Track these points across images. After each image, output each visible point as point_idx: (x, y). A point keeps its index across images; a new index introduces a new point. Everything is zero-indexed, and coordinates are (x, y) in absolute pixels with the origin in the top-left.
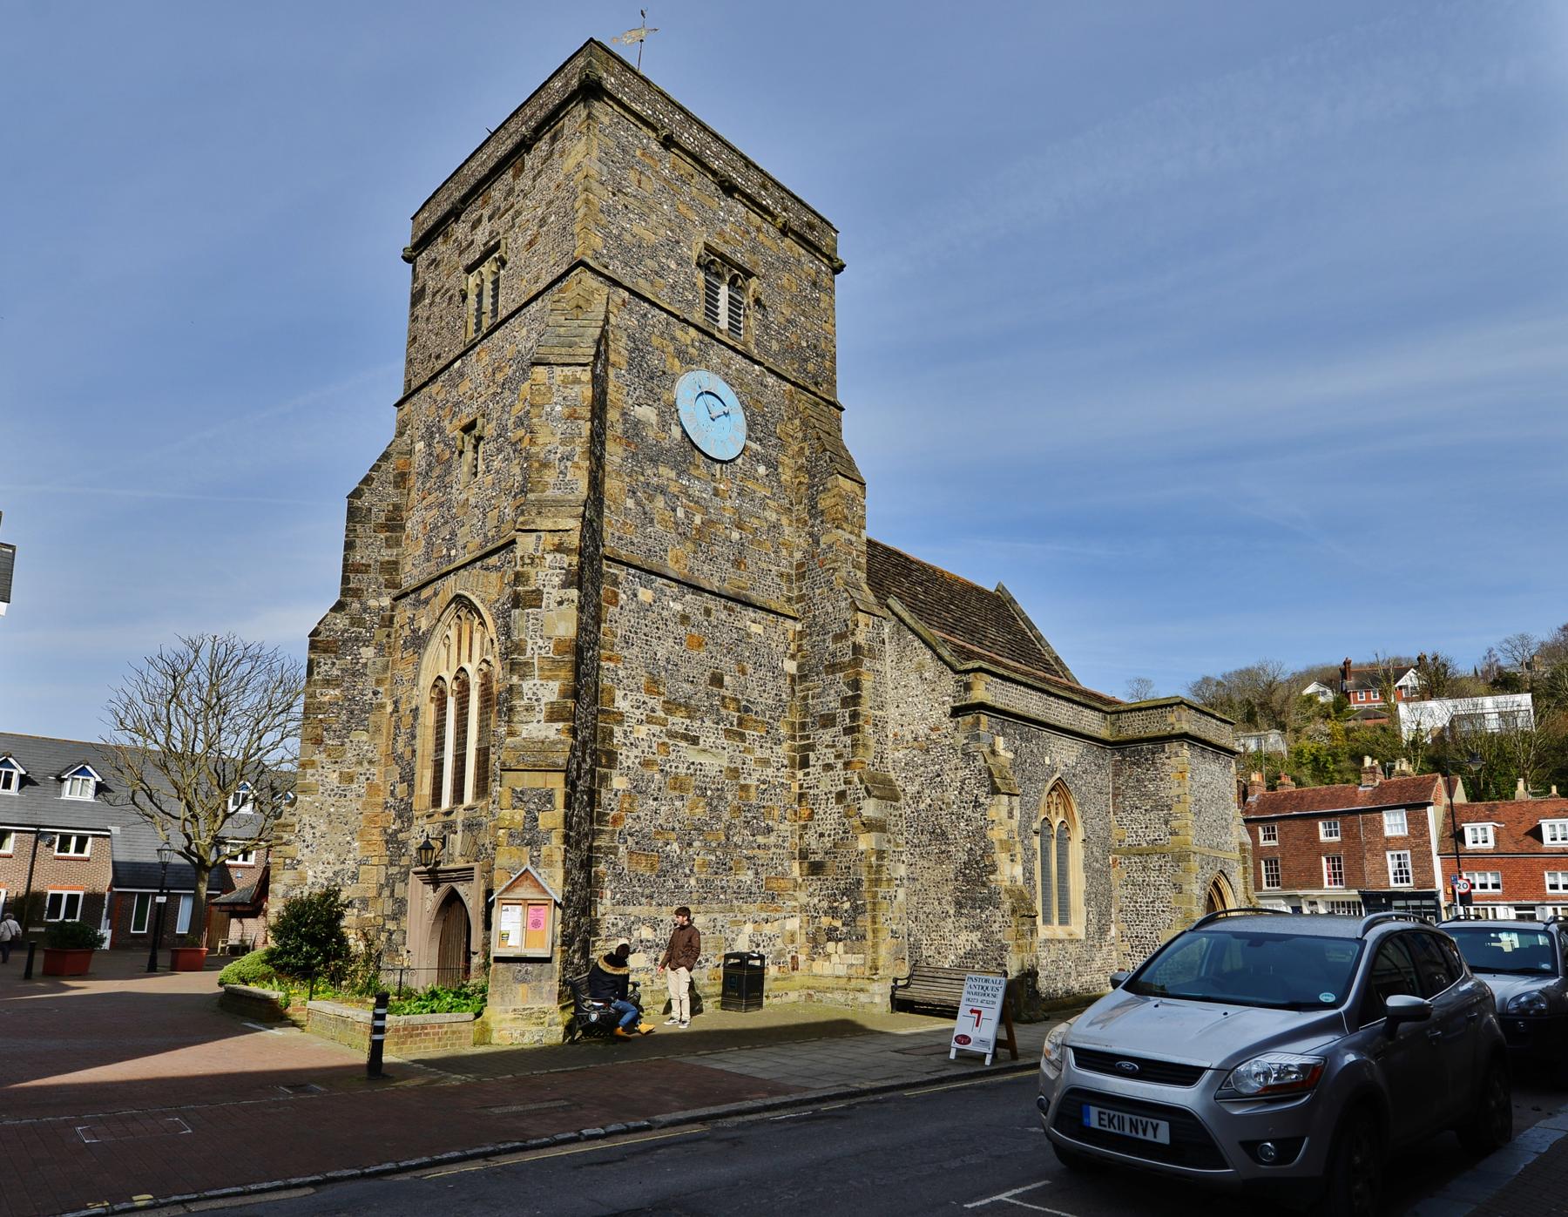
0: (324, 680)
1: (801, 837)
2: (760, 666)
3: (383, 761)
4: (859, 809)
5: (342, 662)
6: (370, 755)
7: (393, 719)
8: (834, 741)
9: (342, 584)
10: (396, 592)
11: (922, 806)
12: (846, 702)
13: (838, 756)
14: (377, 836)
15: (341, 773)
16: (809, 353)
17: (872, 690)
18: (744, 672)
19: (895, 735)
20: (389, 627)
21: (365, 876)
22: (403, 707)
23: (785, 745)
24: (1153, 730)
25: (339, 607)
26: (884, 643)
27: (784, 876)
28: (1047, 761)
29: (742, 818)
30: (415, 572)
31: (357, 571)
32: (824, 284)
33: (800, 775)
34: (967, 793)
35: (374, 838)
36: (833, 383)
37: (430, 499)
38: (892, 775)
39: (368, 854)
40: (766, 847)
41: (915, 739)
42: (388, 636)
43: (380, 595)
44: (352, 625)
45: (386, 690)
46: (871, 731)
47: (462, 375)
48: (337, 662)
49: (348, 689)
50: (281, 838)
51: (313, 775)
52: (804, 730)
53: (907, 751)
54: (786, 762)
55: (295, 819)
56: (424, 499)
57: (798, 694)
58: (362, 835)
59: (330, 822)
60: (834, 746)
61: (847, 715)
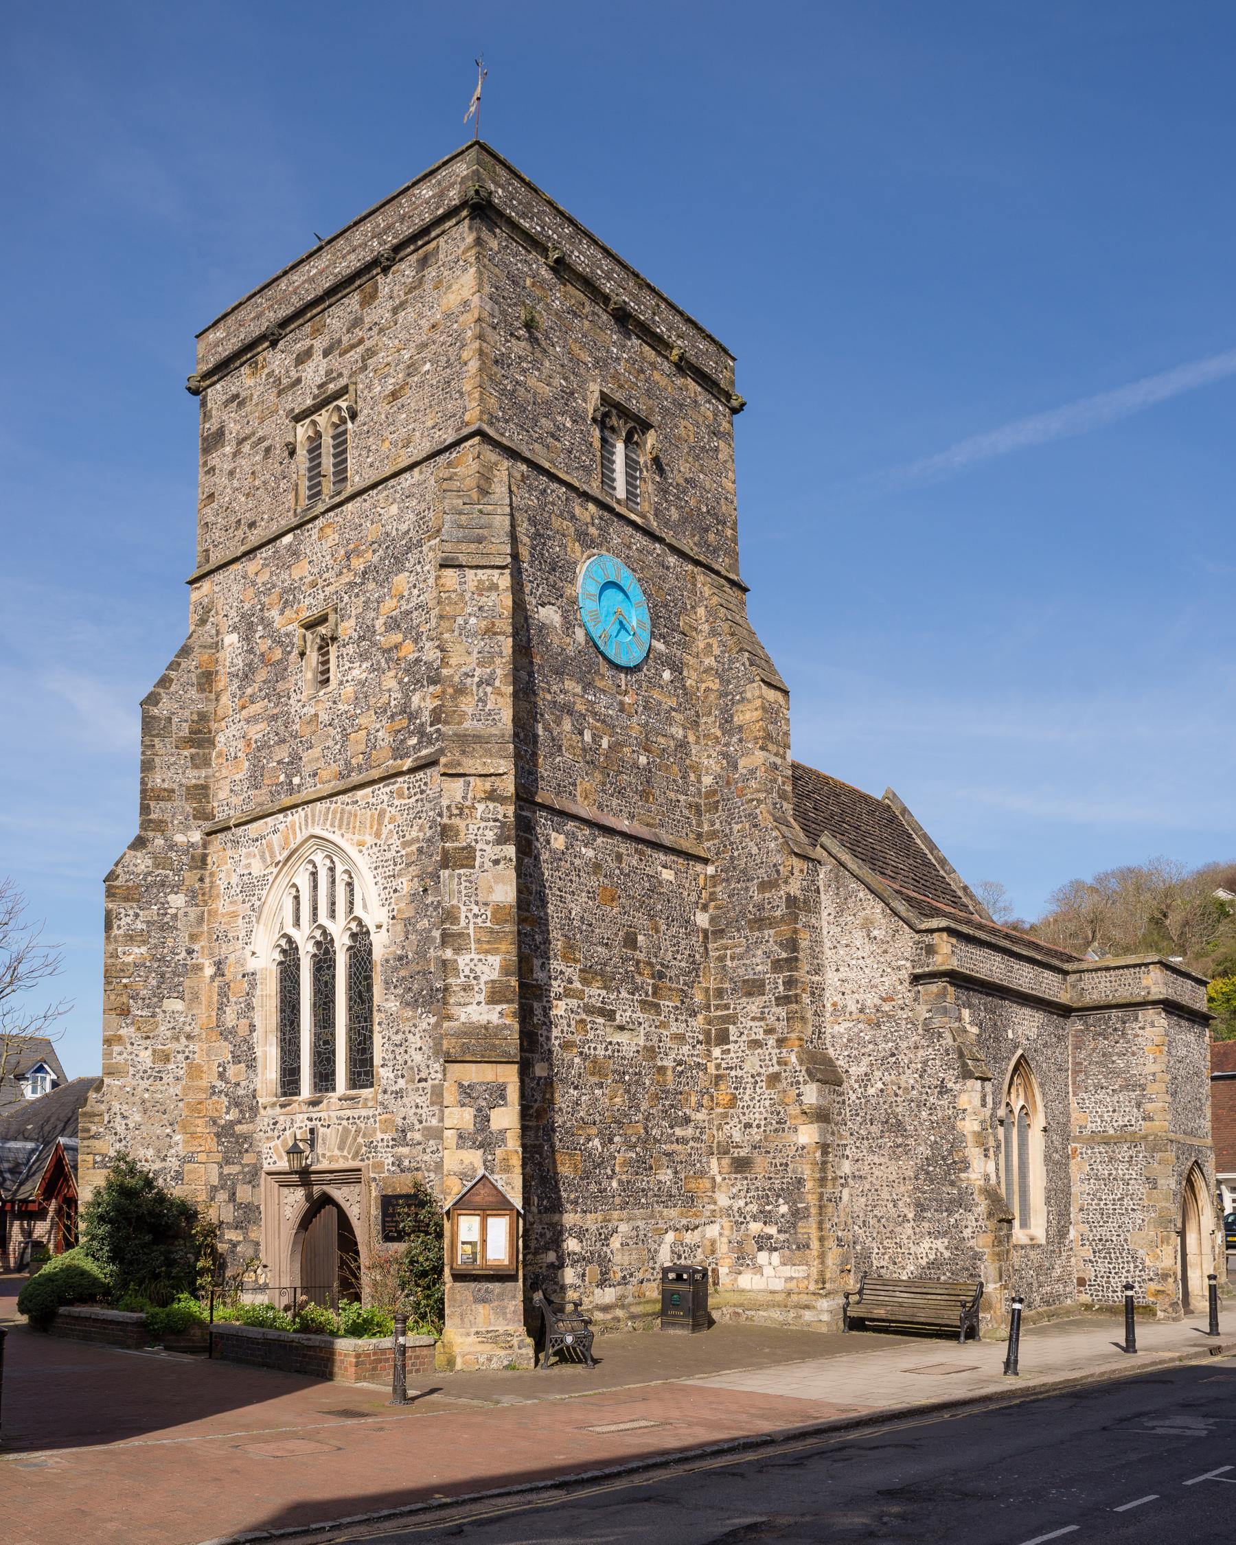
0: (126, 935)
1: (720, 1128)
2: (673, 921)
3: (204, 1036)
4: (798, 1095)
5: (147, 912)
6: (188, 1028)
7: (216, 984)
8: (763, 1013)
9: (141, 814)
10: (208, 826)
11: (871, 1091)
12: (777, 966)
13: (769, 1031)
14: (201, 1127)
15: (154, 1051)
16: (709, 520)
17: (809, 951)
18: (657, 931)
19: (834, 1005)
20: (202, 868)
21: (191, 1177)
22: (230, 972)
23: (700, 1017)
24: (1124, 995)
25: (139, 843)
26: (819, 893)
27: (702, 1174)
28: (1011, 1036)
29: (660, 1107)
30: (235, 800)
31: (158, 799)
32: (722, 429)
33: (717, 1052)
34: (929, 1076)
36: (733, 555)
38: (831, 1051)
39: (193, 1149)
40: (683, 1141)
41: (861, 1011)
42: (201, 880)
43: (188, 828)
44: (157, 866)
45: (202, 947)
46: (808, 1001)
47: (295, 554)
48: (141, 913)
49: (156, 947)
50: (88, 1130)
51: (120, 1054)
52: (722, 998)
53: (851, 1025)
54: (701, 1037)
55: (103, 1107)
56: (244, 707)
57: (711, 954)
58: (184, 1127)
59: (145, 1112)
60: (762, 1019)
61: (780, 981)
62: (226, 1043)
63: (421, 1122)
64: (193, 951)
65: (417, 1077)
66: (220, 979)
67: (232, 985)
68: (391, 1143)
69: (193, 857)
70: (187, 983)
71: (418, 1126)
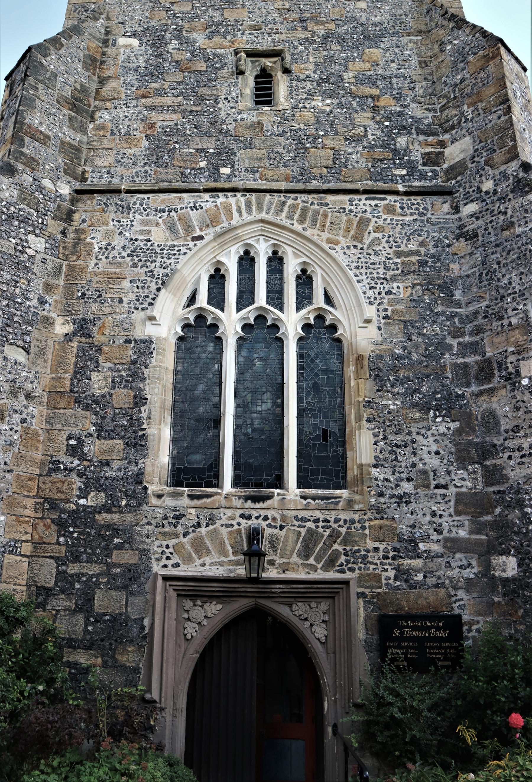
10: (78, 186)
20: (66, 222)
21: (10, 573)
35: (27, 512)
37: (168, 101)
39: (17, 536)
44: (23, 200)
56: (144, 96)
62: (88, 413)
63: (439, 531)
64: (46, 302)
65: (433, 483)
66: (83, 339)
67: (105, 349)
68: (391, 554)
69: (59, 207)
70: (35, 334)
71: (435, 537)
